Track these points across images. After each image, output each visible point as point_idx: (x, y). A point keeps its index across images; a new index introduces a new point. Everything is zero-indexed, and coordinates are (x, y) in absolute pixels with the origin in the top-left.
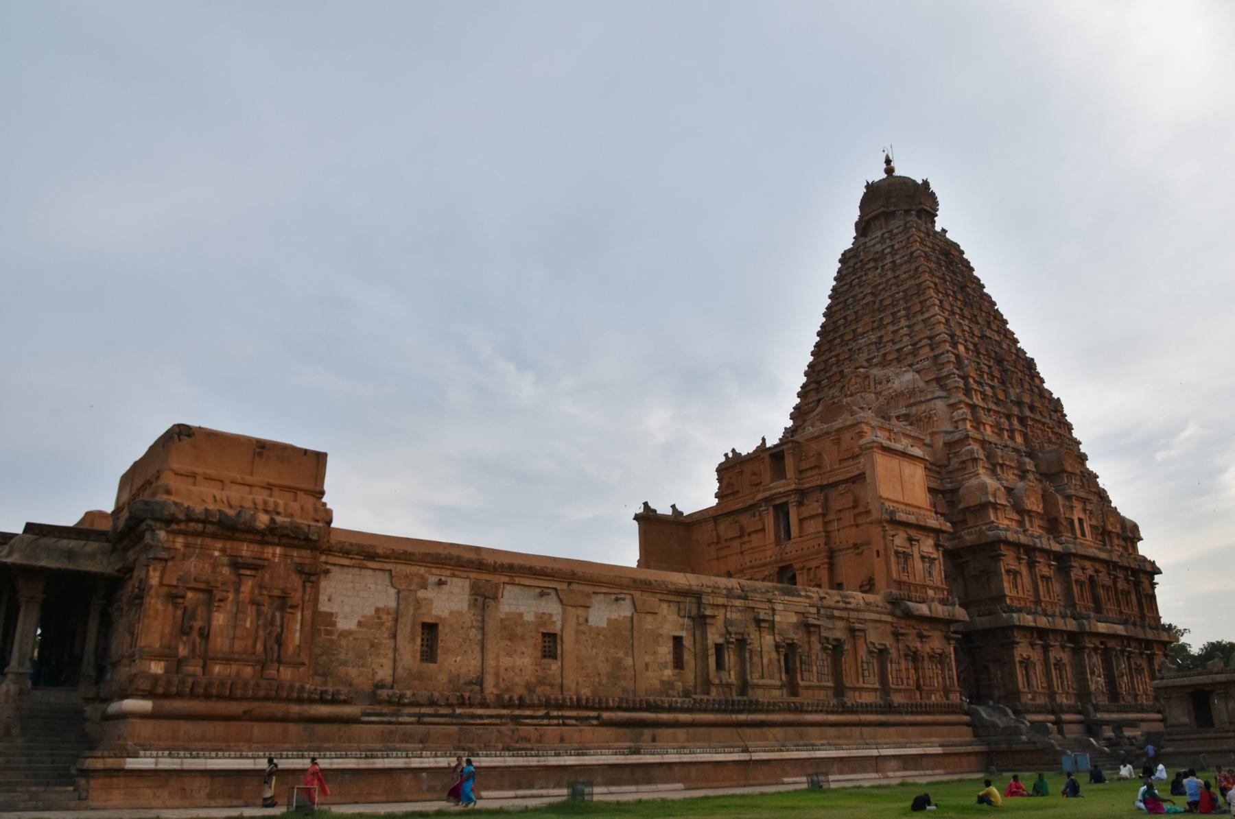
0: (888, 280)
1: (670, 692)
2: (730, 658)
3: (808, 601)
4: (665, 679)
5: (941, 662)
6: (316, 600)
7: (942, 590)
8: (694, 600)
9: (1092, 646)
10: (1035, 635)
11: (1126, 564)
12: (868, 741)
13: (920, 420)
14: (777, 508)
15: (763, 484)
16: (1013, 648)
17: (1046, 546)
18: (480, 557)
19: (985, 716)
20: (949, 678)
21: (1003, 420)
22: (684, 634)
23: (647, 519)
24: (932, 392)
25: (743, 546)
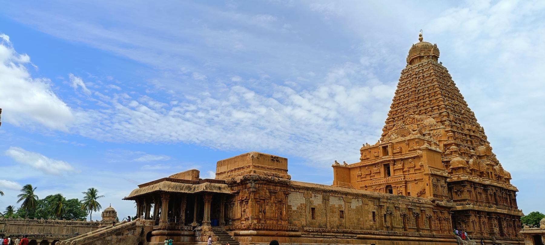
2: (388, 218)
3: (409, 201)
8: (378, 200)
9: (495, 217)
14: (384, 165)
16: (470, 217)
22: (375, 211)
23: (337, 167)
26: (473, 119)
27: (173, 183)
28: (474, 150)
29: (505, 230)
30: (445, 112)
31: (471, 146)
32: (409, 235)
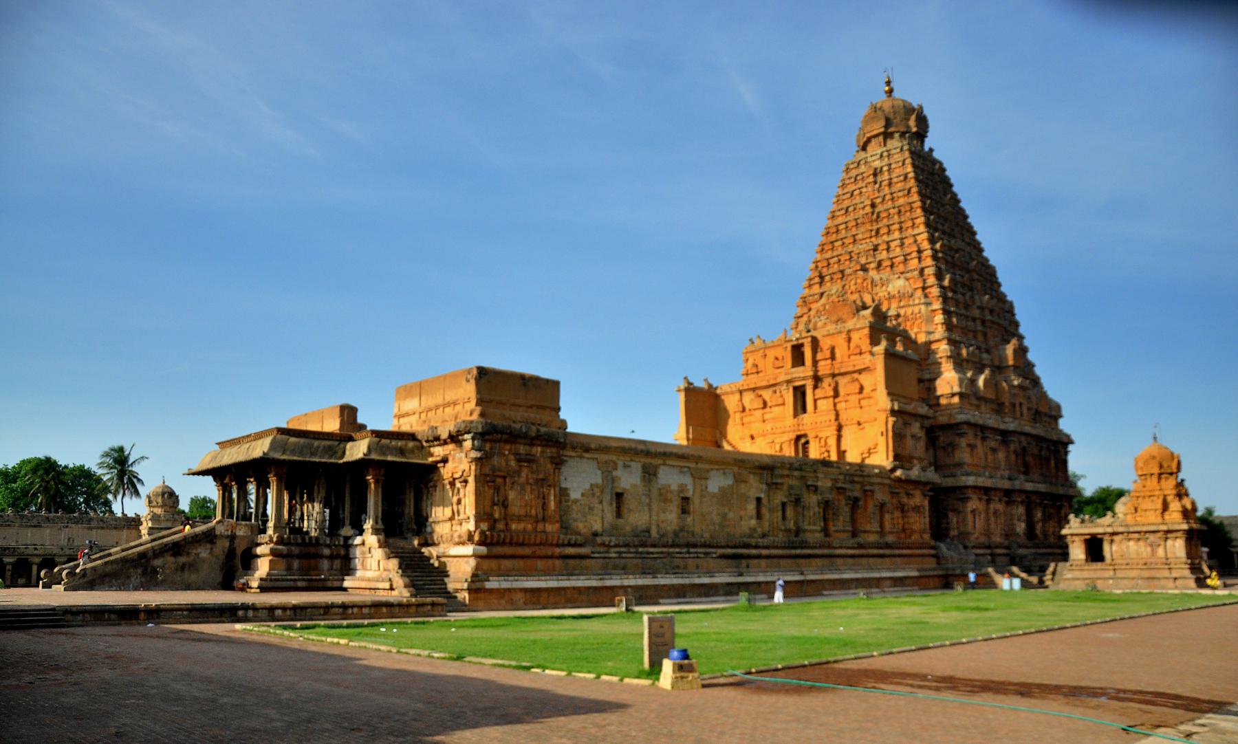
1: (755, 535)
2: (790, 512)
3: (838, 470)
4: (752, 526)
5: (919, 512)
6: (559, 481)
10: (983, 492)
11: (1050, 437)
14: (795, 388)
17: (996, 426)
21: (970, 323)
22: (762, 495)
27: (293, 439)
29: (1039, 527)
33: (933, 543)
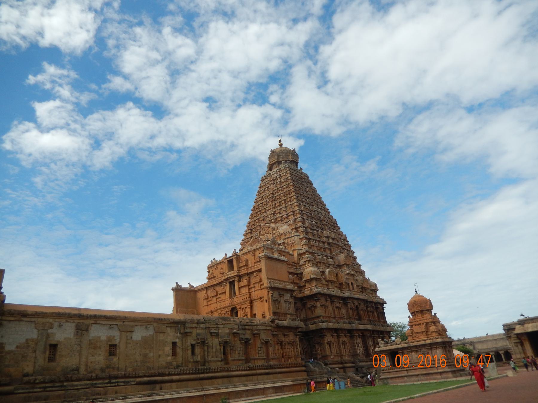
0: (278, 189)
1: (170, 367)
2: (197, 350)
3: (234, 323)
4: (168, 361)
7: (294, 315)
8: (182, 326)
9: (357, 334)
11: (372, 300)
12: (260, 382)
13: (289, 244)
15: (225, 273)
17: (338, 295)
18: (80, 313)
19: (311, 366)
20: (297, 352)
21: (321, 244)
22: (177, 341)
23: (178, 290)
24: (294, 233)
25: (218, 300)
26: (335, 227)
28: (333, 259)
30: (299, 217)
31: (329, 255)
32: (232, 369)
33: (303, 363)
